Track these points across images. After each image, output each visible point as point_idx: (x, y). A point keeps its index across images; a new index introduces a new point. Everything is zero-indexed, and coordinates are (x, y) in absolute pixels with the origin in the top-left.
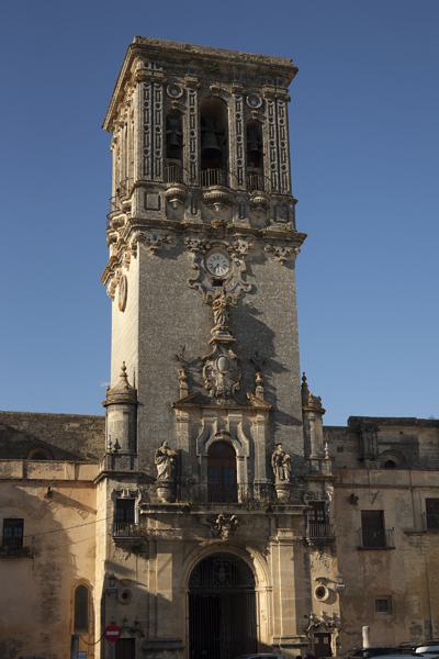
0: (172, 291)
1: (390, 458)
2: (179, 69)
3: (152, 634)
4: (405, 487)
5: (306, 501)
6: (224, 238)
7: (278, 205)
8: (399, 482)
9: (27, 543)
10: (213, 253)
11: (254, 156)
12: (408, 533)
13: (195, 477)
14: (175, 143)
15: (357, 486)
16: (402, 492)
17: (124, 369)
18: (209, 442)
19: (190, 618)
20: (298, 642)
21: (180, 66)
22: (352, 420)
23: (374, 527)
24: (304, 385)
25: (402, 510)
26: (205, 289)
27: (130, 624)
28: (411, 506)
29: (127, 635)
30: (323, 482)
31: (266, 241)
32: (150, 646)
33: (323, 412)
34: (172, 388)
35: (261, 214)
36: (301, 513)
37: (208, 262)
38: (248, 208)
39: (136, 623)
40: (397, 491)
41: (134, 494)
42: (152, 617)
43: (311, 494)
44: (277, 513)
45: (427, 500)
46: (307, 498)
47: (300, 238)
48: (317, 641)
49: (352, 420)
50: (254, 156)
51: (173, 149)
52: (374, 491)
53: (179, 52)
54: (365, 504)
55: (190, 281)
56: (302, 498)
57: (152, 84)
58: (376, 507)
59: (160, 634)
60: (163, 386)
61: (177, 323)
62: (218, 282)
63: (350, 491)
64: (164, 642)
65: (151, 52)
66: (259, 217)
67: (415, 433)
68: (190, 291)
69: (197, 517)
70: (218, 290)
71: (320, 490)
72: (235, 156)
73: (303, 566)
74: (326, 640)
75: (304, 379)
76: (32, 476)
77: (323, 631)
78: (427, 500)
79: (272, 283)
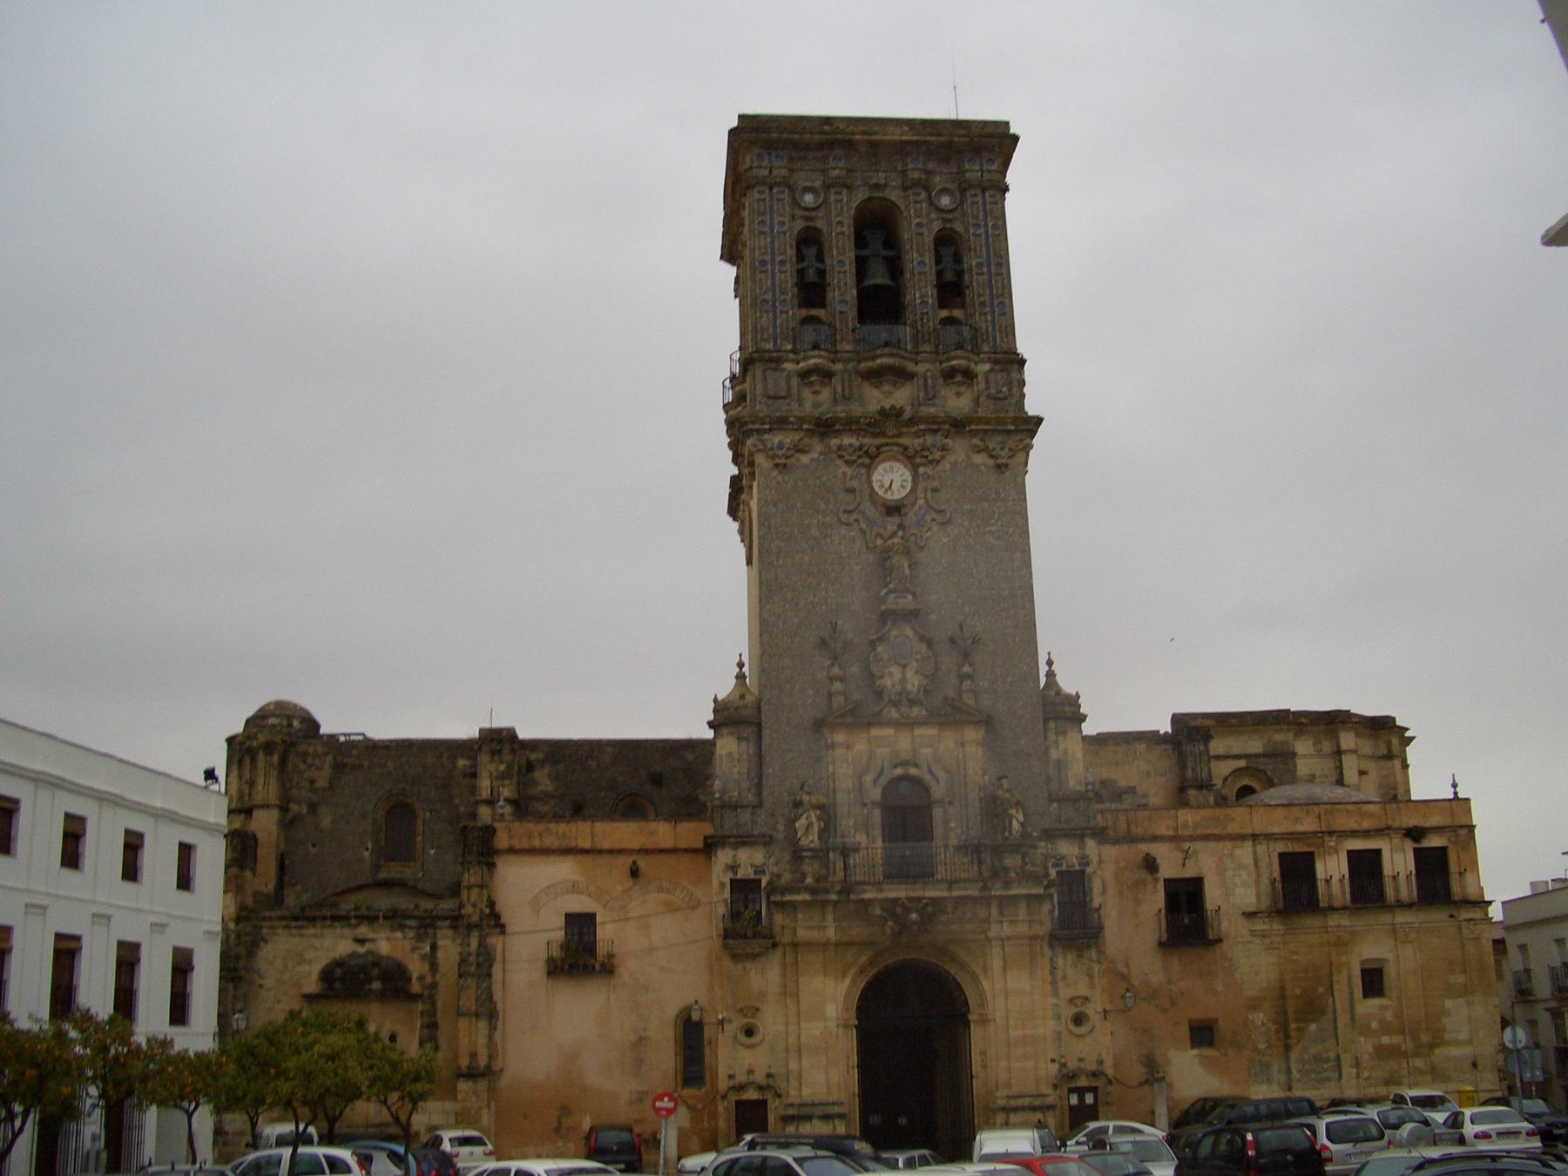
1: (1246, 781)
3: (793, 1092)
4: (1242, 837)
5: (1053, 873)
6: (900, 435)
7: (991, 370)
8: (1232, 828)
9: (602, 949)
10: (884, 461)
11: (951, 290)
12: (1249, 915)
13: (861, 838)
15: (1155, 839)
18: (883, 781)
19: (861, 1066)
20: (1038, 1102)
22: (1177, 719)
23: (1185, 901)
24: (1051, 675)
26: (871, 523)
27: (759, 1077)
29: (752, 1095)
30: (1081, 837)
31: (973, 433)
32: (791, 1112)
33: (1083, 718)
35: (962, 389)
36: (1040, 891)
37: (875, 477)
38: (941, 381)
39: (769, 1075)
40: (1228, 844)
41: (759, 870)
42: (793, 1066)
43: (1059, 859)
44: (999, 893)
45: (1281, 855)
47: (1039, 421)
48: (1074, 1100)
49: (1177, 719)
50: (951, 290)
51: (812, 292)
52: (1186, 845)
54: (1170, 866)
56: (1046, 867)
58: (1189, 873)
59: (807, 1093)
62: (893, 509)
63: (1144, 848)
64: (814, 1105)
66: (958, 394)
67: (1290, 736)
68: (843, 530)
69: (867, 903)
70: (892, 523)
71: (1076, 851)
72: (920, 291)
73: (1050, 979)
74: (1089, 1099)
75: (1050, 663)
77: (1082, 1082)
78: (1281, 855)
79: (986, 504)
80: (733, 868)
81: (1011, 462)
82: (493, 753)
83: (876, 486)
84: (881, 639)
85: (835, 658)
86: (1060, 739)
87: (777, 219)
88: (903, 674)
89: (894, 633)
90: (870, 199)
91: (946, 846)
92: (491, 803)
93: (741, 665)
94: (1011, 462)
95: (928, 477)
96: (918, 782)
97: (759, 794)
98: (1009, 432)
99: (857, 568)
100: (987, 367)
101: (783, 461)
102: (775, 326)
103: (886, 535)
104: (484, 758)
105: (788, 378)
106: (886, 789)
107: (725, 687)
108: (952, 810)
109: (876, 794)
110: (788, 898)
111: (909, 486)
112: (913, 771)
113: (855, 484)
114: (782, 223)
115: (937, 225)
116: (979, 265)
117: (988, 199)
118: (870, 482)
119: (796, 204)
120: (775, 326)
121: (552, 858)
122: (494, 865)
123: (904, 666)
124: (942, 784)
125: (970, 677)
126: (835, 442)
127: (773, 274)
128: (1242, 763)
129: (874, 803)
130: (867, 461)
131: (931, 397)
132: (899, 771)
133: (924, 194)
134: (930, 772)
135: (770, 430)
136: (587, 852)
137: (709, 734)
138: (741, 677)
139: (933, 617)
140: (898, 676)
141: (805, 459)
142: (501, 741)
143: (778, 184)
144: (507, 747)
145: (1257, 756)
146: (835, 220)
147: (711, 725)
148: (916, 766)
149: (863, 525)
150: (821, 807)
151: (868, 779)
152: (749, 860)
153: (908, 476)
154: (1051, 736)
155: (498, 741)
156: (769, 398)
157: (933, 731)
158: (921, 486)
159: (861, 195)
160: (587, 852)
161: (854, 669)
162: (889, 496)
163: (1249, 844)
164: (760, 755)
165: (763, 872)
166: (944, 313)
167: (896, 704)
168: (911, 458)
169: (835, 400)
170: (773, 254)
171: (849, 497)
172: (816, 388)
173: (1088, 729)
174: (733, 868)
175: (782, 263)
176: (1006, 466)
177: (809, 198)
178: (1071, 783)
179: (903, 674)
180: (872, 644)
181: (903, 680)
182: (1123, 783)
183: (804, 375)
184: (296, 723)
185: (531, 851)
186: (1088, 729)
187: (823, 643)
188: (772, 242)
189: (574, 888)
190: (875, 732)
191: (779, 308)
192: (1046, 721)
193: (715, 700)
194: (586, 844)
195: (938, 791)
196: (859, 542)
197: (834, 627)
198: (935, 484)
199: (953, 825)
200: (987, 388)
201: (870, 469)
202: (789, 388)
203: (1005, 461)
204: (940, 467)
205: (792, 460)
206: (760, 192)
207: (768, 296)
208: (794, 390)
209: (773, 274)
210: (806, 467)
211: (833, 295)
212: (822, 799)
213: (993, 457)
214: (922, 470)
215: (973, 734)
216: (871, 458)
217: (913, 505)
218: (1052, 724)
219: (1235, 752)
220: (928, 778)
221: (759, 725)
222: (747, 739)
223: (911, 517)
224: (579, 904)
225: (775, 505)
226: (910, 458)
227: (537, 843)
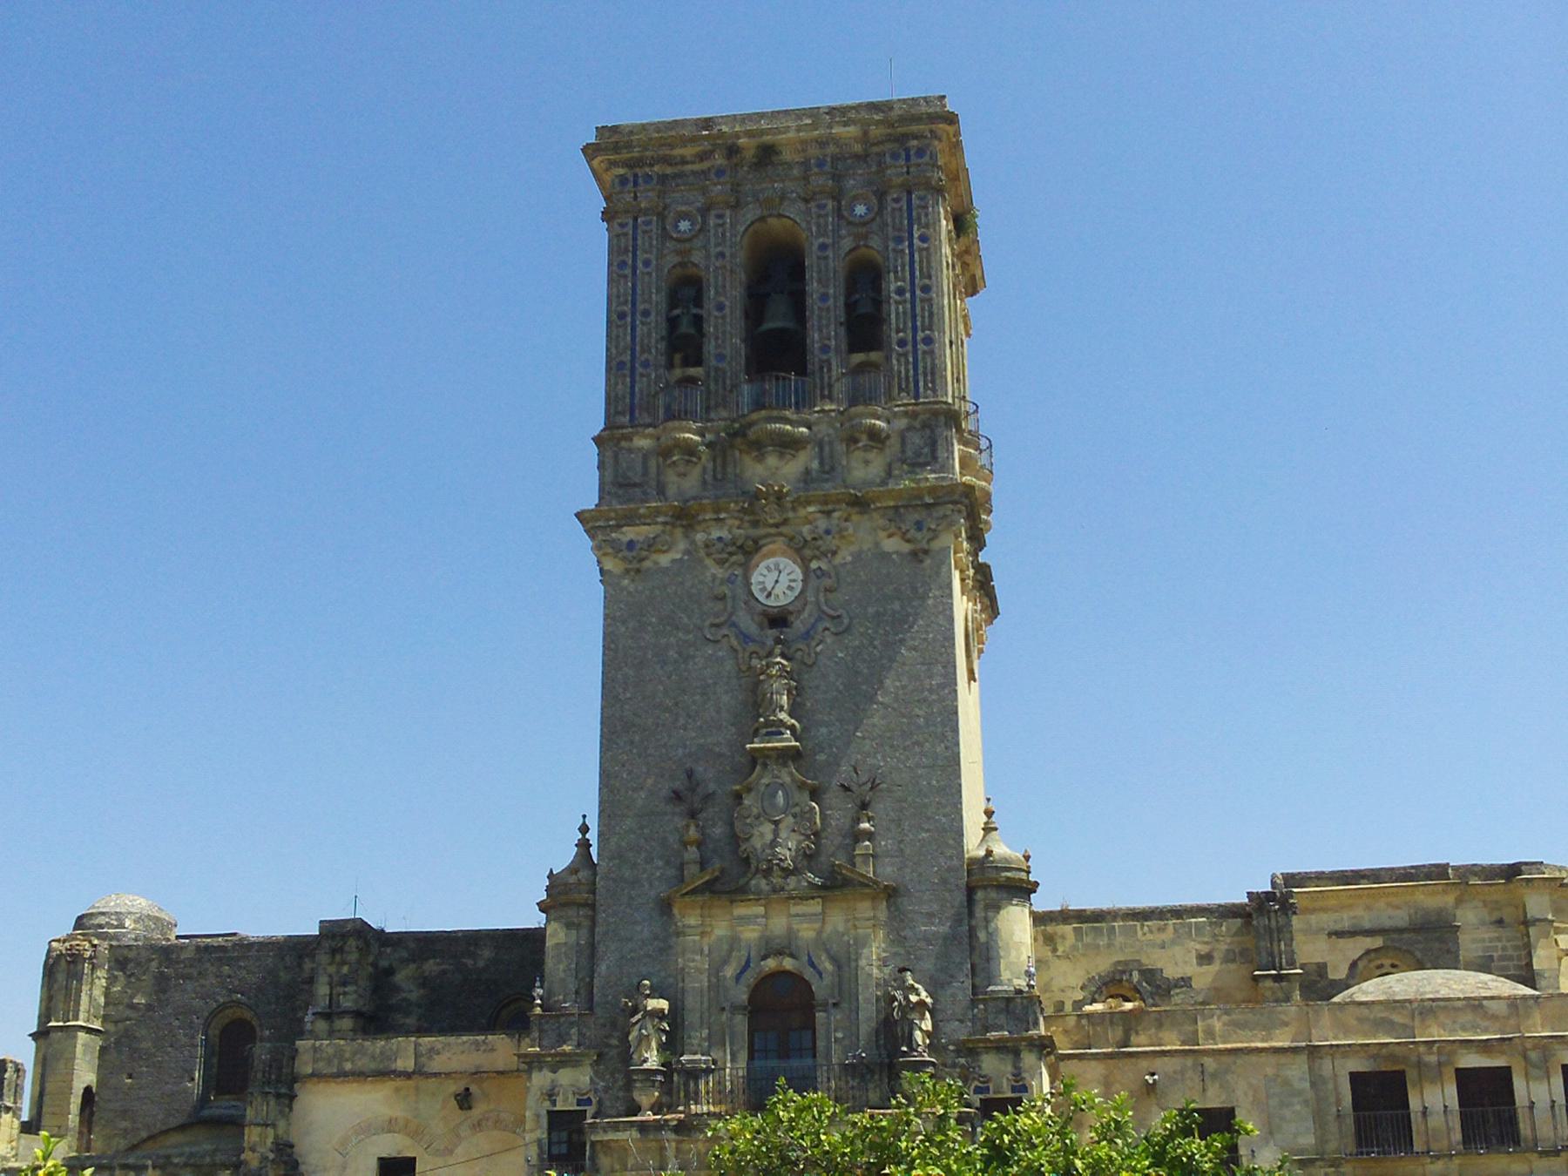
0: (672, 654)
2: (693, 173)
6: (785, 522)
7: (910, 428)
10: (766, 556)
14: (685, 328)
16: (1283, 1059)
17: (584, 829)
18: (750, 978)
21: (697, 167)
25: (1282, 1105)
26: (745, 638)
28: (1310, 1094)
30: (1016, 1053)
34: (668, 863)
35: (872, 455)
37: (755, 578)
38: (841, 448)
46: (978, 1090)
50: (865, 328)
53: (685, 141)
55: (713, 625)
57: (635, 219)
60: (649, 860)
61: (682, 721)
62: (778, 619)
65: (625, 155)
66: (867, 462)
71: (1010, 1068)
76: (436, 1065)
79: (897, 606)
80: (551, 1095)
81: (936, 545)
82: (334, 952)
83: (755, 589)
84: (749, 790)
85: (693, 815)
86: (990, 914)
87: (641, 256)
88: (776, 833)
89: (765, 781)
90: (762, 219)
91: (829, 1065)
92: (328, 1016)
93: (584, 829)
94: (936, 545)
95: (820, 573)
96: (794, 980)
97: (591, 999)
98: (928, 506)
99: (725, 698)
100: (902, 423)
101: (635, 565)
102: (632, 394)
103: (763, 653)
104: (323, 958)
105: (645, 457)
106: (755, 991)
107: (563, 858)
108: (837, 1016)
109: (742, 996)
110: (611, 1136)
111: (798, 586)
112: (788, 964)
113: (725, 589)
114: (647, 263)
115: (847, 243)
116: (900, 291)
117: (915, 202)
118: (748, 584)
119: (665, 235)
120: (632, 394)
121: (368, 1087)
122: (292, 1097)
123: (776, 823)
124: (827, 980)
125: (869, 836)
126: (700, 537)
127: (633, 329)
128: (1378, 942)
129: (735, 1008)
130: (739, 558)
131: (829, 469)
132: (771, 964)
133: (830, 204)
134: (812, 964)
135: (619, 526)
136: (408, 1075)
137: (536, 920)
138: (584, 845)
139: (821, 757)
140: (769, 837)
141: (664, 560)
142: (344, 936)
143: (646, 212)
144: (352, 943)
145: (1400, 931)
146: (714, 251)
147: (543, 907)
148: (792, 956)
149: (735, 643)
150: (658, 1014)
151: (729, 972)
152: (575, 1081)
153: (798, 574)
154: (979, 912)
155: (345, 936)
156: (621, 486)
157: (815, 907)
158: (813, 582)
159: (751, 213)
160: (408, 1075)
161: (718, 831)
162: (771, 602)
163: (1303, 1058)
164: (593, 946)
165: (589, 1102)
166: (858, 358)
167: (767, 873)
168: (801, 550)
169: (704, 482)
170: (634, 304)
171: (719, 606)
172: (681, 469)
173: (1043, 901)
174: (551, 1095)
175: (646, 313)
176: (926, 552)
177: (684, 225)
178: (1005, 975)
179: (776, 833)
180: (738, 797)
181: (774, 844)
182: (1171, 972)
183: (665, 453)
184: (127, 923)
185: (342, 1076)
186: (1043, 901)
187: (677, 796)
188: (634, 286)
189: (390, 1126)
190: (741, 910)
191: (640, 370)
192: (971, 891)
193: (551, 875)
194: (406, 1063)
195: (820, 988)
196: (729, 665)
197: (690, 774)
198: (827, 582)
199: (840, 1037)
200: (903, 452)
201: (747, 570)
202: (645, 473)
203: (924, 545)
204: (838, 560)
205: (647, 564)
206: (622, 225)
207: (627, 358)
208: (653, 470)
209: (633, 329)
210: (665, 571)
211: (710, 348)
212: (664, 1004)
213: (908, 541)
214: (814, 565)
215: (864, 908)
216: (749, 551)
217: (800, 612)
218: (980, 895)
219: (1367, 925)
220: (808, 974)
221: (593, 907)
222: (578, 926)
223: (798, 625)
224: (393, 1145)
225: (624, 622)
226: (798, 551)
227: (348, 1066)
